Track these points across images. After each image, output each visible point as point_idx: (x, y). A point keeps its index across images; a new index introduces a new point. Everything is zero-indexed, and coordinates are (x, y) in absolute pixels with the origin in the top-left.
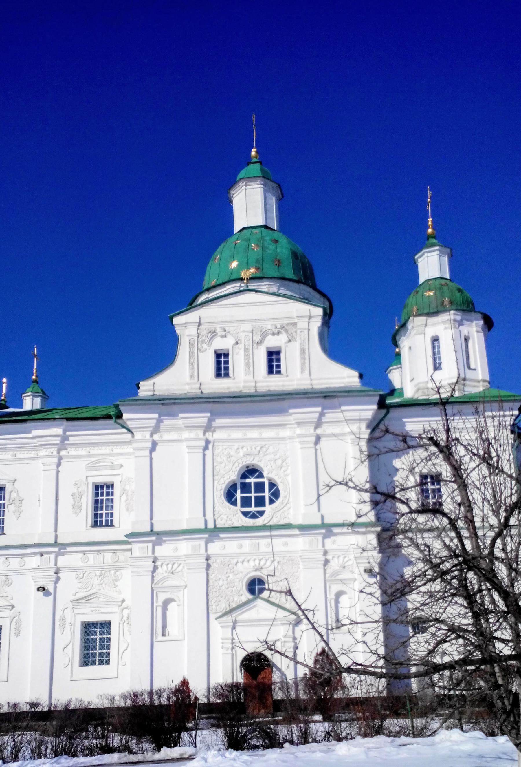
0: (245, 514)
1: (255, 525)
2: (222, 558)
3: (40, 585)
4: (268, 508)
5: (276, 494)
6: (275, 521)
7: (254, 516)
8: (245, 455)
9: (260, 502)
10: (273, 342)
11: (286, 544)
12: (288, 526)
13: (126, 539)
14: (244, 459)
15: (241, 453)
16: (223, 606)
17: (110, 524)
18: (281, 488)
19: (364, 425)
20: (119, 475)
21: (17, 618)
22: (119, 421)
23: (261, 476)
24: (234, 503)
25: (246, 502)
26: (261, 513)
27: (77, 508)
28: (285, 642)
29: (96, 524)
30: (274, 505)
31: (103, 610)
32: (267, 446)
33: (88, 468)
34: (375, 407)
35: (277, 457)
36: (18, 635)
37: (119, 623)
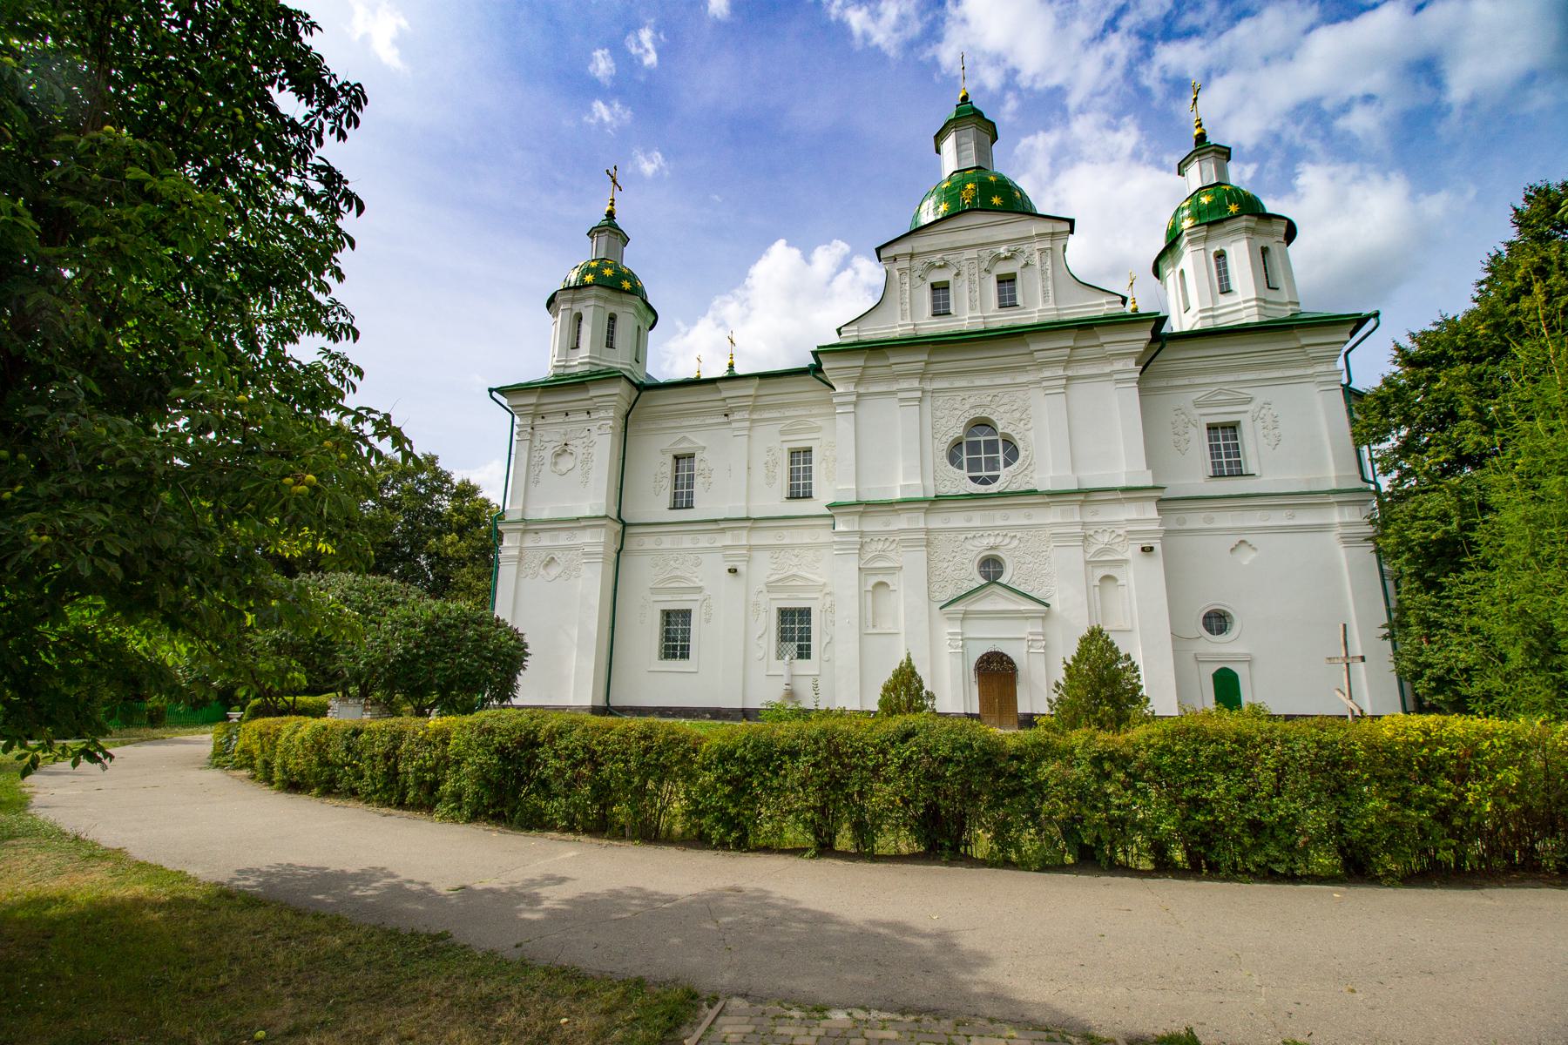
0: (974, 479)
3: (730, 565)
4: (1004, 473)
5: (1012, 453)
6: (1013, 488)
7: (985, 481)
8: (972, 408)
9: (992, 464)
10: (1005, 268)
11: (1029, 516)
12: (1032, 492)
13: (828, 512)
14: (972, 412)
15: (967, 406)
16: (950, 593)
17: (808, 496)
18: (1020, 445)
19: (1131, 364)
22: (820, 376)
23: (994, 431)
24: (960, 467)
25: (974, 465)
26: (995, 479)
29: (793, 496)
30: (1011, 468)
31: (802, 595)
33: (782, 433)
34: (1149, 336)
36: (708, 621)
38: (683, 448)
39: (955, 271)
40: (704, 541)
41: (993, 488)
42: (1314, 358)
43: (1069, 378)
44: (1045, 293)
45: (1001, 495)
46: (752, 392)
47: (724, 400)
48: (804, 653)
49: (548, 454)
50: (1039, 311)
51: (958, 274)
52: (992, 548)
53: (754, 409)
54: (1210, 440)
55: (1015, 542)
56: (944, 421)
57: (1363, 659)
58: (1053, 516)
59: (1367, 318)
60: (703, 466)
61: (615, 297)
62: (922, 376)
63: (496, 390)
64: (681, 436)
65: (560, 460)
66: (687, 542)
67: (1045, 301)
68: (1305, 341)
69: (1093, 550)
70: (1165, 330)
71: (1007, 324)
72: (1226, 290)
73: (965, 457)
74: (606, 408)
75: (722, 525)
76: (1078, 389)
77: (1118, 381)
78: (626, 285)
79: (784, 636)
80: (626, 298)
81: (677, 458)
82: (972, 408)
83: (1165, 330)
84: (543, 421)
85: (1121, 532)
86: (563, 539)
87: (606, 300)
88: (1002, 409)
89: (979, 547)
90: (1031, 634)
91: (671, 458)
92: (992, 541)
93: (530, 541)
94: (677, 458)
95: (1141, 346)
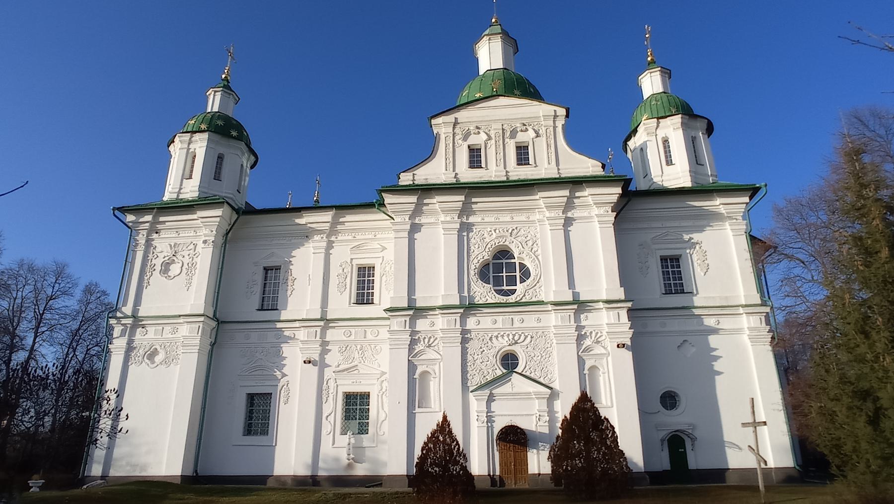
0: (499, 292)
1: (508, 302)
2: (476, 333)
4: (520, 287)
9: (512, 281)
11: (539, 320)
13: (385, 315)
15: (494, 235)
17: (370, 302)
20: (380, 257)
21: (285, 386)
25: (497, 282)
27: (342, 287)
30: (525, 284)
32: (518, 228)
35: (528, 238)
37: (378, 396)
38: (270, 263)
41: (512, 299)
45: (518, 304)
48: (363, 429)
54: (663, 268)
57: (765, 423)
61: (224, 141)
63: (118, 209)
70: (632, 188)
71: (522, 178)
72: (669, 162)
73: (491, 275)
78: (234, 133)
79: (348, 415)
80: (233, 143)
81: (266, 269)
83: (632, 188)
89: (502, 344)
91: (262, 269)
94: (266, 269)
95: (615, 198)
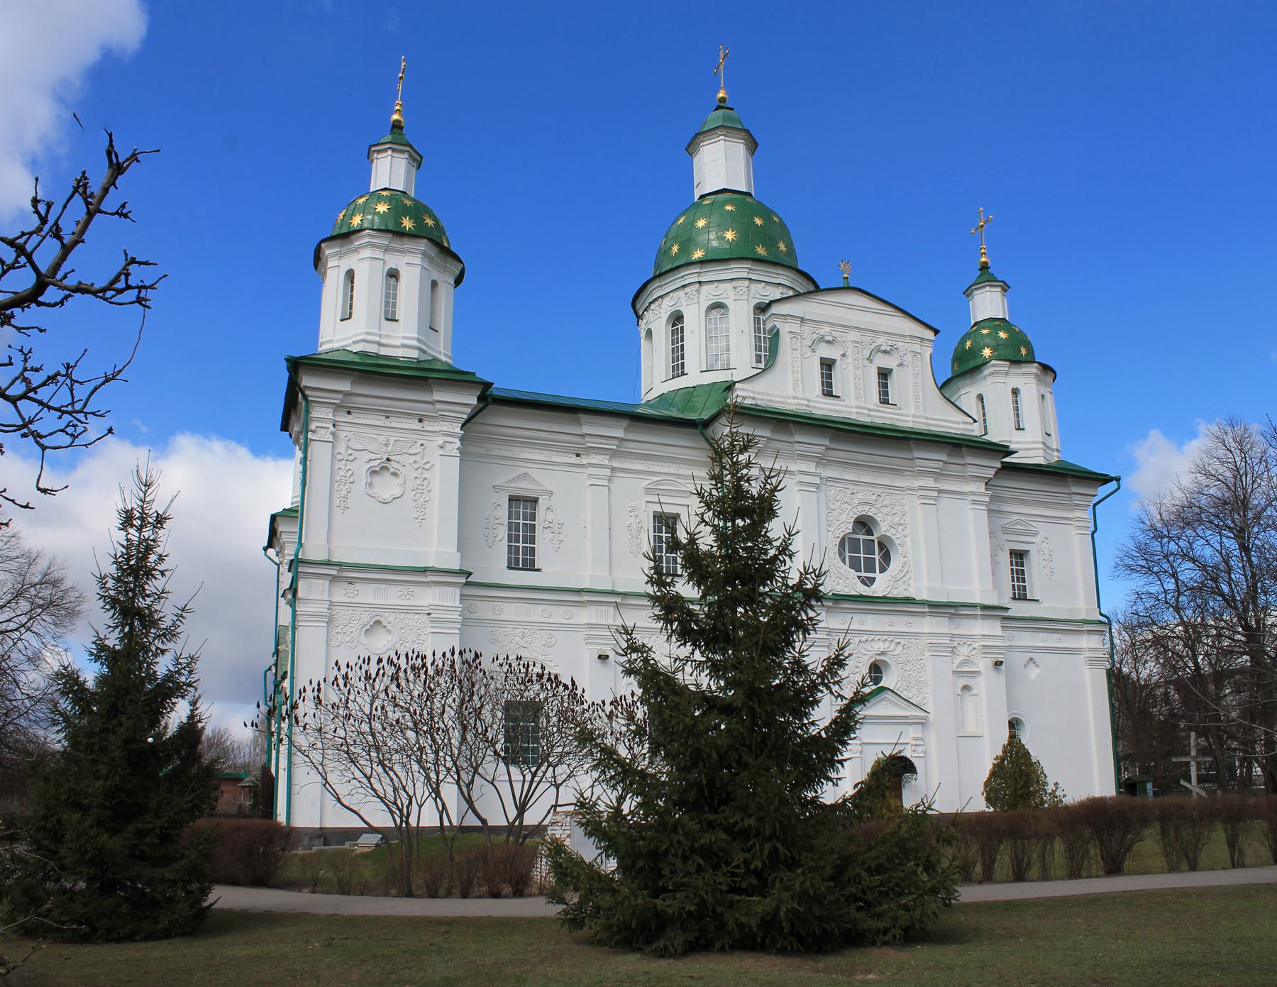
8: (860, 504)
9: (870, 567)
12: (909, 601)
14: (860, 508)
15: (856, 501)
28: (916, 745)
38: (524, 488)
39: (842, 352)
40: (558, 614)
42: (1077, 505)
43: (940, 491)
44: (917, 398)
46: (620, 434)
47: (583, 436)
49: (361, 468)
50: (914, 416)
51: (844, 355)
52: (883, 653)
53: (614, 454)
55: (900, 648)
56: (836, 513)
58: (929, 625)
59: (1112, 479)
60: (550, 517)
62: (820, 461)
64: (521, 471)
65: (377, 480)
66: (537, 613)
67: (917, 407)
68: (1074, 490)
69: (958, 660)
74: (445, 418)
75: (586, 598)
76: (946, 502)
77: (975, 502)
82: (860, 504)
84: (349, 419)
85: (975, 645)
86: (394, 595)
87: (387, 249)
88: (885, 510)
90: (915, 739)
92: (880, 646)
93: (341, 594)
